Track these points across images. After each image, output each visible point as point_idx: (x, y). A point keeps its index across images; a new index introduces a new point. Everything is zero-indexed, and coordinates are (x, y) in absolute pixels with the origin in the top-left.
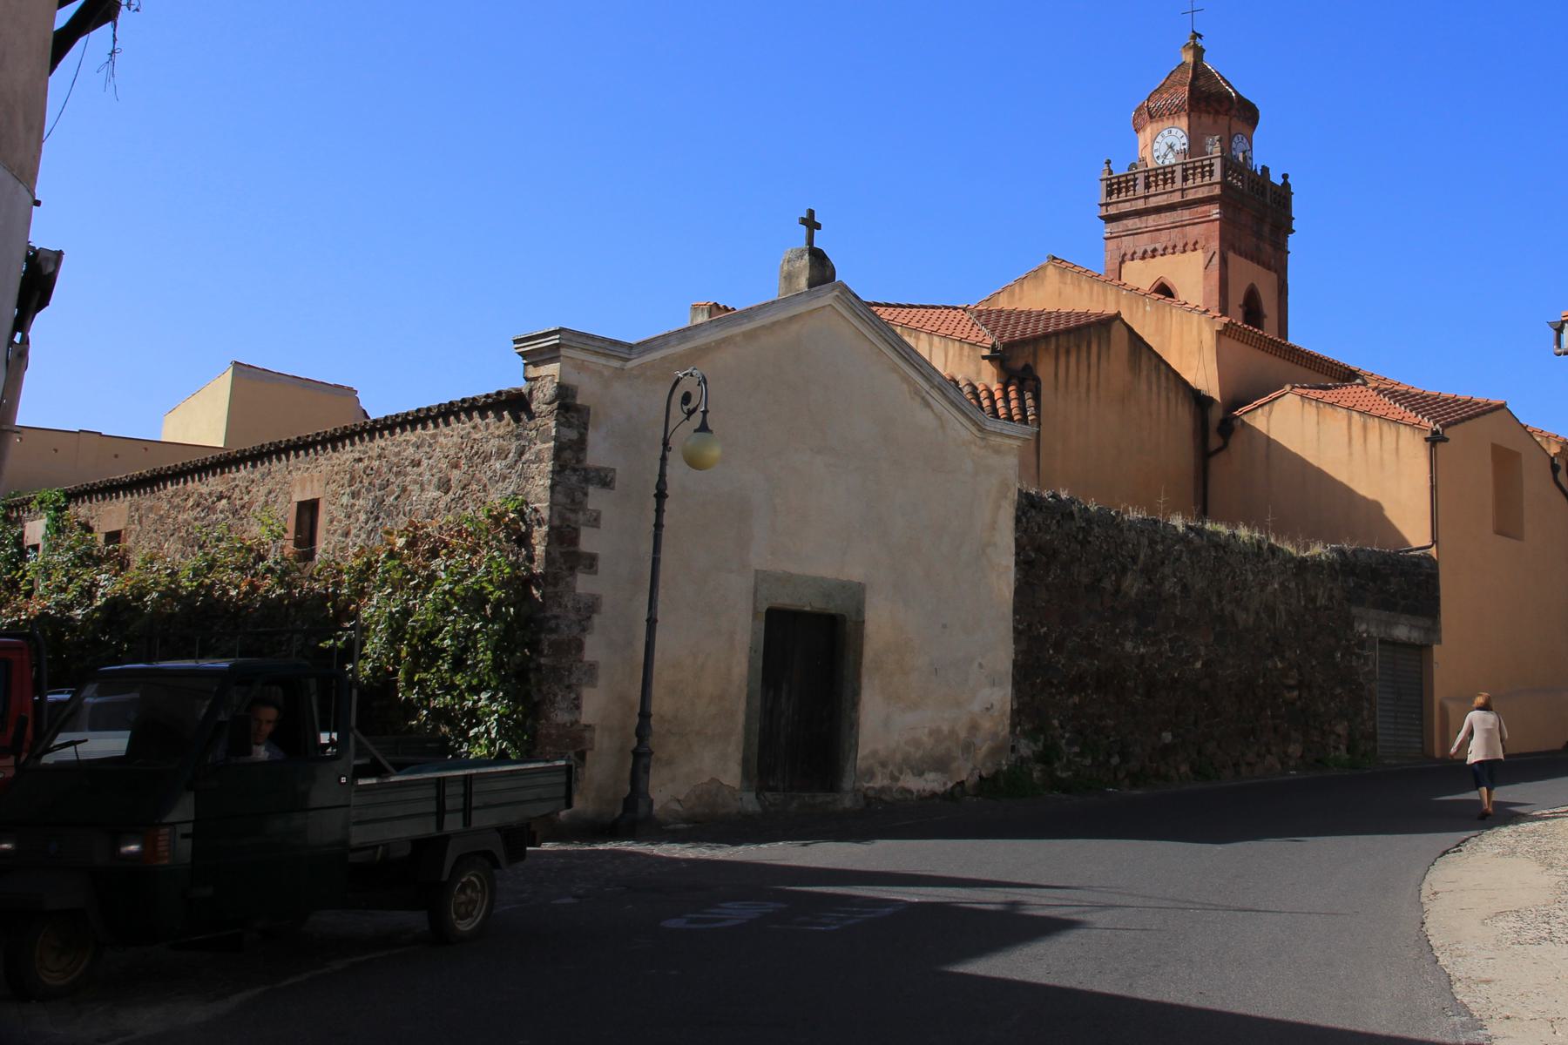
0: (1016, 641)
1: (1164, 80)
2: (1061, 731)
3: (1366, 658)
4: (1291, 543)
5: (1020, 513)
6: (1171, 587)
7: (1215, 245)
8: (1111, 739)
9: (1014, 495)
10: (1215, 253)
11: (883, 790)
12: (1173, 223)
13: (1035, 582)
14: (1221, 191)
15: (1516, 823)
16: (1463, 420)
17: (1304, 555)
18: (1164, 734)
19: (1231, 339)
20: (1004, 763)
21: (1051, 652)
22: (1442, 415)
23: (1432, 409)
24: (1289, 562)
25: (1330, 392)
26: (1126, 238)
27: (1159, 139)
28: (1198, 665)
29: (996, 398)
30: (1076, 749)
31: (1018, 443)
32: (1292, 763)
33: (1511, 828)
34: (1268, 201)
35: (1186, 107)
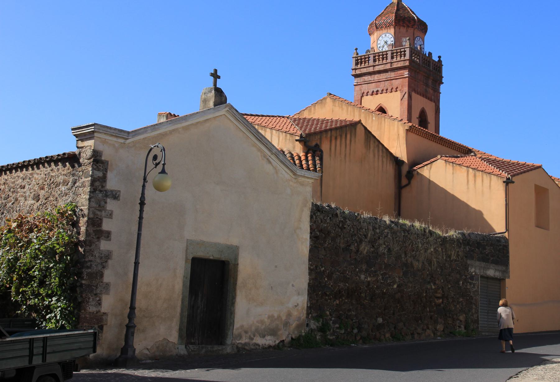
0: (310, 274)
1: (383, 11)
2: (330, 317)
3: (474, 285)
4: (440, 230)
5: (312, 214)
6: (382, 250)
7: (406, 89)
8: (354, 321)
9: (310, 205)
10: (406, 93)
11: (245, 344)
12: (387, 78)
13: (319, 246)
14: (409, 63)
15: (545, 364)
16: (521, 173)
17: (445, 236)
18: (378, 319)
19: (412, 133)
20: (303, 332)
21: (326, 279)
22: (512, 171)
23: (516, 167)
24: (439, 238)
25: (459, 159)
26: (364, 85)
27: (381, 38)
28: (395, 286)
29: (302, 160)
30: (337, 325)
31: (312, 181)
32: (439, 334)
33: (542, 366)
34: (431, 69)
35: (393, 24)
